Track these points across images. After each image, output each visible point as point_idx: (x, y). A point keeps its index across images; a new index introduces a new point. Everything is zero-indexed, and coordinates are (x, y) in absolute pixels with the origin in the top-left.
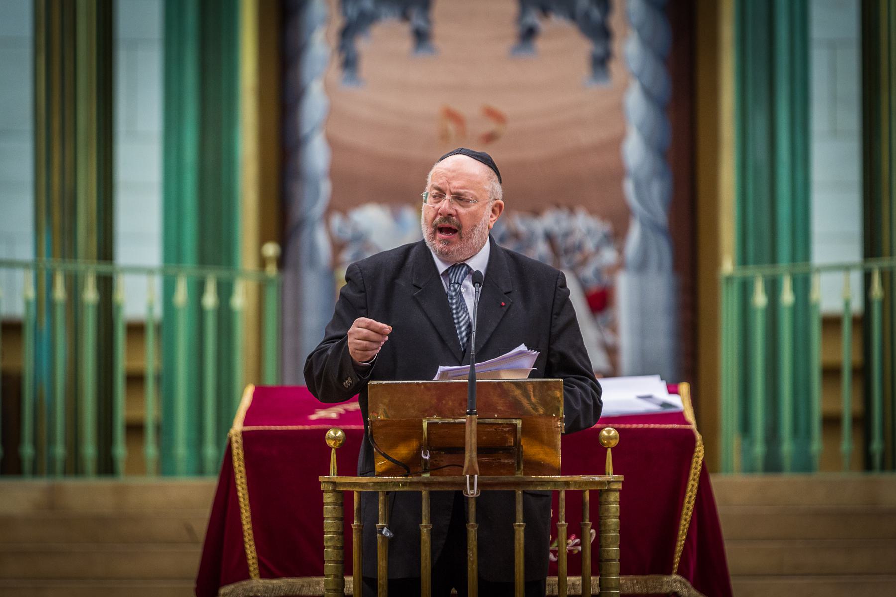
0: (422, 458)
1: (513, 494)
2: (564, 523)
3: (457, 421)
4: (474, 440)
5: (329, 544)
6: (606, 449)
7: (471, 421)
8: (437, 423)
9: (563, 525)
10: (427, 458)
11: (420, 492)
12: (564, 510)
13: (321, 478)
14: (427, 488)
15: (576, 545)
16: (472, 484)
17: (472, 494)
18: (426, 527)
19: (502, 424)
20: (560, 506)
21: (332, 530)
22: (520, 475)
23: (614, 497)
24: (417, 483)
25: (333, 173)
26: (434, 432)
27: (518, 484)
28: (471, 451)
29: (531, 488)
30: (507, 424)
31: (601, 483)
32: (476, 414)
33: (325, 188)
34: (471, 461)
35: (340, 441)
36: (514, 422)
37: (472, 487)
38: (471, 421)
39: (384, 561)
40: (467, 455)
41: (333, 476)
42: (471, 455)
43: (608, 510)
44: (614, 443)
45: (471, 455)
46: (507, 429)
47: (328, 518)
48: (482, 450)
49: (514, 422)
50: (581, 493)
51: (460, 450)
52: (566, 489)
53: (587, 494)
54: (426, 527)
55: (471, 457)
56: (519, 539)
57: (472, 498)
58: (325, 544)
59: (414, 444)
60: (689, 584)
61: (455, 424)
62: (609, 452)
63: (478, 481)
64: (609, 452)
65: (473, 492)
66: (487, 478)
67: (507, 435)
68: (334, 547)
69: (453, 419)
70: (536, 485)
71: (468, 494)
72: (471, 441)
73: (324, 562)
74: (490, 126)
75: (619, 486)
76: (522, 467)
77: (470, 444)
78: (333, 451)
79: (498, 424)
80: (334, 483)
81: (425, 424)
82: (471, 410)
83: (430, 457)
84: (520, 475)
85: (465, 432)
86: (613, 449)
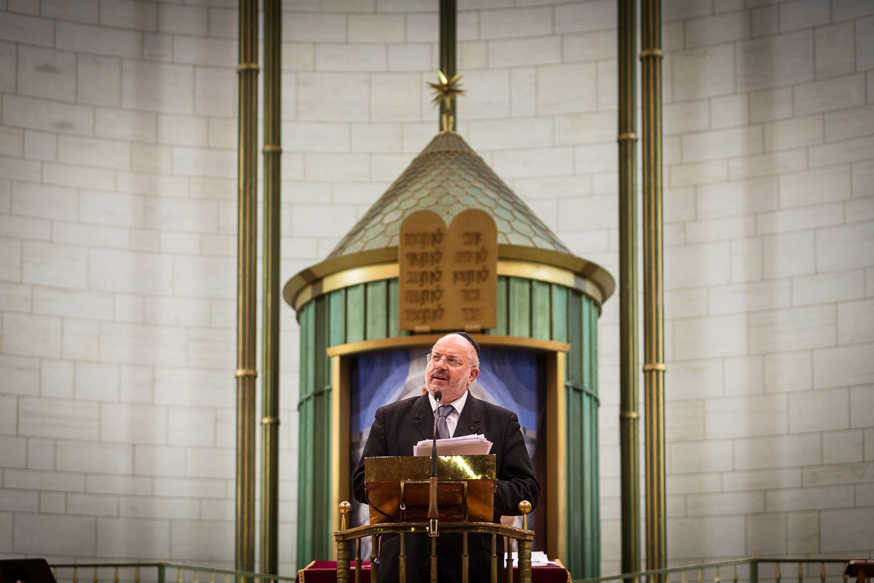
0: (401, 509)
1: (461, 535)
2: (495, 555)
3: (424, 482)
5: (340, 576)
7: (433, 481)
8: (410, 484)
9: (494, 557)
10: (404, 509)
11: (399, 534)
12: (495, 547)
14: (404, 531)
17: (434, 534)
18: (403, 556)
19: (454, 484)
20: (493, 544)
21: (342, 566)
26: (409, 493)
28: (433, 501)
29: (474, 531)
30: (458, 484)
32: (436, 476)
34: (433, 508)
35: (348, 509)
36: (462, 482)
37: (434, 530)
38: (433, 481)
39: (375, 581)
46: (457, 490)
49: (462, 482)
52: (496, 532)
54: (403, 556)
55: (433, 505)
56: (465, 565)
57: (434, 537)
58: (338, 576)
59: (396, 502)
61: (423, 484)
63: (438, 526)
65: (434, 533)
66: (444, 524)
67: (457, 495)
68: (344, 578)
69: (422, 481)
71: (431, 535)
76: (467, 518)
77: (432, 497)
79: (451, 484)
81: (402, 485)
82: (434, 474)
83: (406, 509)
84: (466, 522)
85: (429, 492)
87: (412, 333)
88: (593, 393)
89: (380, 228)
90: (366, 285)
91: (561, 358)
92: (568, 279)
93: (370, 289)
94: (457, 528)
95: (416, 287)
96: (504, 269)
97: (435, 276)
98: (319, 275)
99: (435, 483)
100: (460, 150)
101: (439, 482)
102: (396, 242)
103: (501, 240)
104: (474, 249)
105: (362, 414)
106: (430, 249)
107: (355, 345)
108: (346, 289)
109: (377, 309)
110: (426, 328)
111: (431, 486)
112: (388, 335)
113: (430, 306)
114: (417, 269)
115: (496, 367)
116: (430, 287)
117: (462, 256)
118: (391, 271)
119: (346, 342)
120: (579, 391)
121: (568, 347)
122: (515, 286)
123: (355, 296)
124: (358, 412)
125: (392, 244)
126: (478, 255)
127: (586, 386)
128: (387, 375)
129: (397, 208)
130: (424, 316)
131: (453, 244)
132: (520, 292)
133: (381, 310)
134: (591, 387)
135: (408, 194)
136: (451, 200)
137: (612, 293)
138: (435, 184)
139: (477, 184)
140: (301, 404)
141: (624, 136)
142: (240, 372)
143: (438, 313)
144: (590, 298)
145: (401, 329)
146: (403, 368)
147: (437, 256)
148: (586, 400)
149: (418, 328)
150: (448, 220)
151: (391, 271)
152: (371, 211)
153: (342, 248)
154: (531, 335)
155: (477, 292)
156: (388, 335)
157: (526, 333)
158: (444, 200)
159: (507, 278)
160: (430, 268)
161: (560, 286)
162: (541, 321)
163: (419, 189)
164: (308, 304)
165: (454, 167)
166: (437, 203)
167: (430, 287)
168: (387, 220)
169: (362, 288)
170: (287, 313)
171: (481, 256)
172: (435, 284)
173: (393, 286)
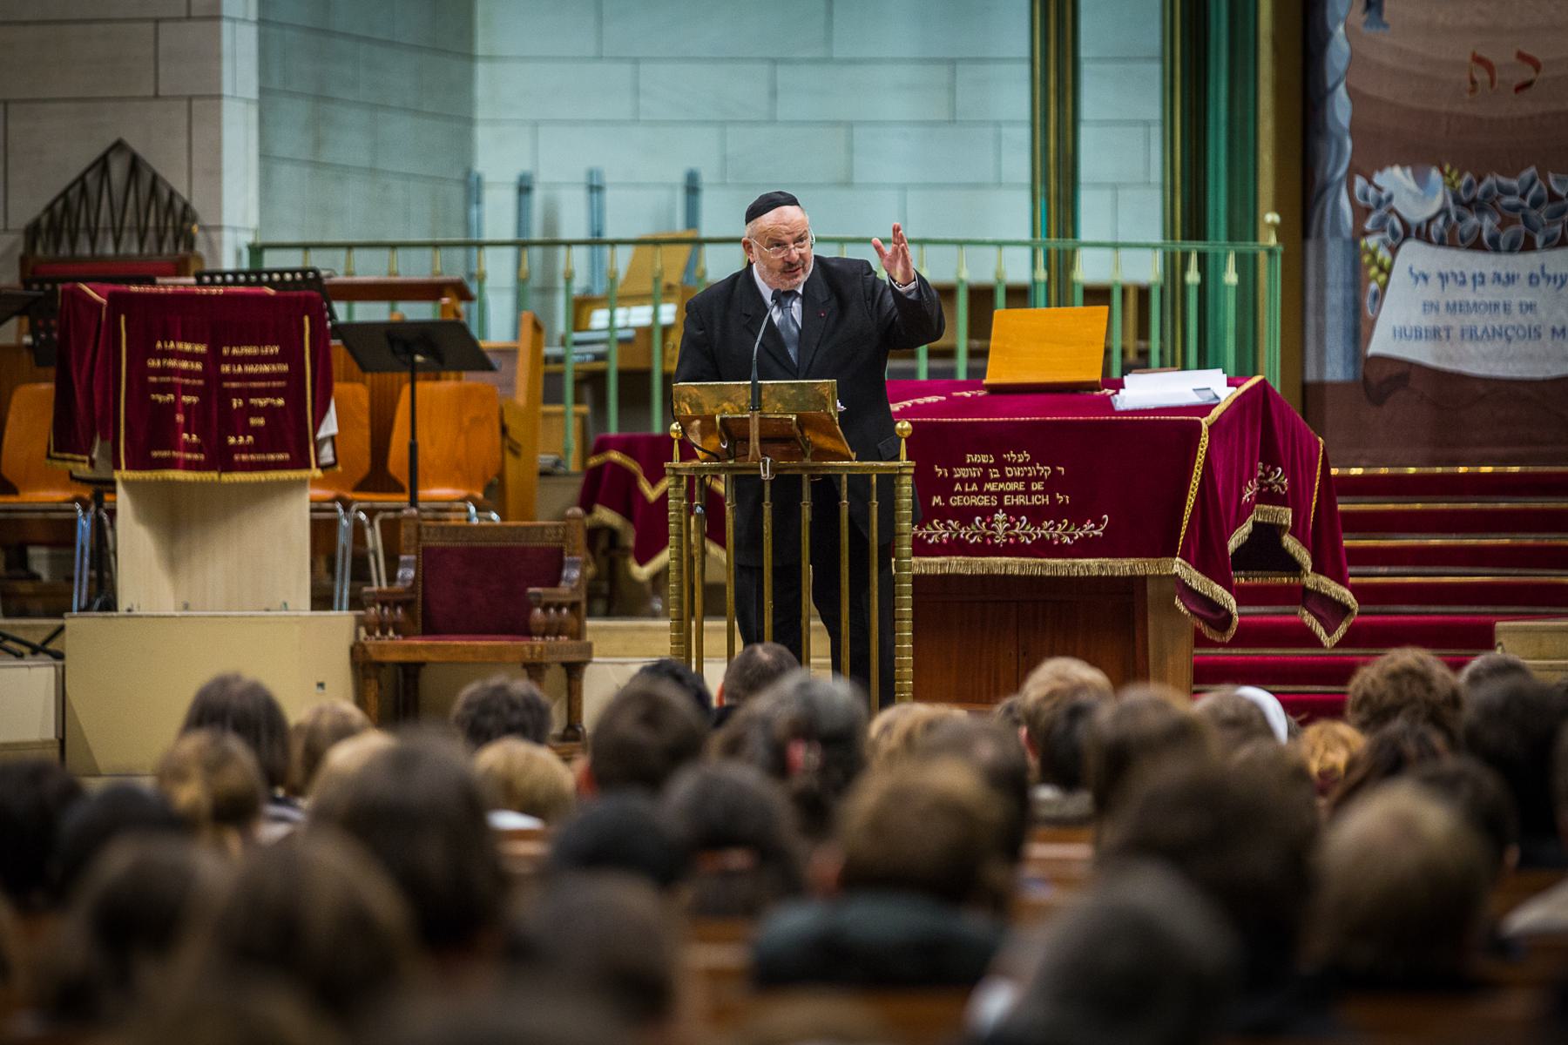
2: (845, 502)
4: (756, 432)
6: (901, 439)
9: (844, 504)
10: (725, 447)
13: (666, 465)
15: (1091, 529)
16: (765, 469)
18: (729, 505)
22: (807, 461)
23: (908, 480)
25: (1354, 131)
33: (1349, 144)
36: (790, 416)
37: (765, 472)
40: (751, 444)
41: (676, 463)
42: (755, 443)
43: (900, 491)
44: (907, 434)
45: (755, 443)
47: (671, 499)
48: (762, 440)
49: (790, 416)
53: (874, 477)
54: (729, 505)
60: (1190, 567)
62: (903, 441)
64: (903, 441)
65: (766, 475)
70: (819, 470)
72: (754, 432)
73: (668, 536)
74: (1528, 73)
75: (912, 471)
78: (676, 442)
80: (674, 469)
81: (718, 419)
82: (754, 407)
83: (728, 447)
84: (807, 461)
86: (907, 440)
99: (756, 419)
101: (763, 416)
111: (751, 421)
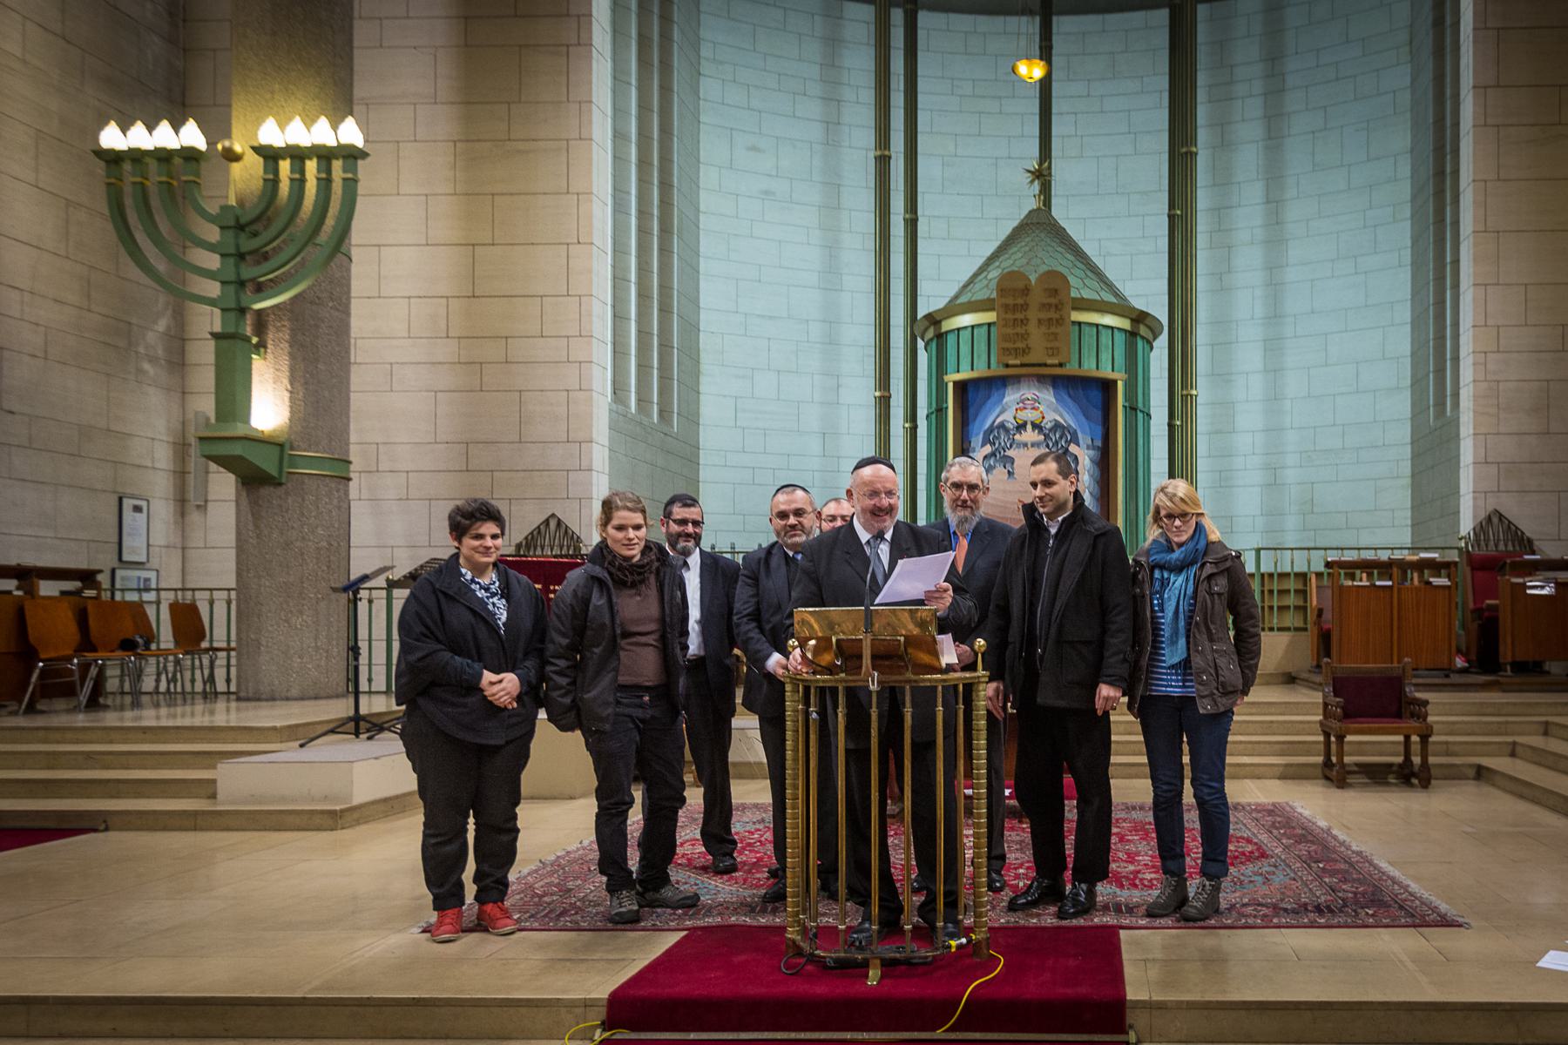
1: (904, 688)
4: (869, 652)
7: (866, 637)
16: (873, 681)
22: (909, 675)
24: (836, 681)
27: (909, 681)
31: (975, 678)
34: (867, 667)
37: (873, 684)
38: (866, 637)
40: (864, 661)
42: (867, 661)
43: (977, 696)
44: (983, 649)
45: (867, 661)
48: (874, 657)
50: (955, 687)
51: (860, 657)
65: (874, 687)
81: (834, 639)
86: (983, 655)
87: (1007, 366)
88: (1146, 410)
89: (985, 282)
90: (973, 327)
91: (1120, 384)
92: (1125, 324)
93: (976, 331)
94: (900, 681)
95: (1010, 331)
96: (1077, 316)
97: (1025, 322)
98: (938, 319)
100: (1047, 222)
102: (994, 295)
103: (1074, 294)
104: (1053, 301)
105: (970, 427)
106: (1020, 301)
107: (965, 375)
108: (959, 329)
109: (981, 347)
110: (1018, 362)
111: (864, 642)
112: (989, 367)
113: (1020, 345)
114: (1010, 316)
115: (1071, 392)
116: (1019, 330)
117: (1045, 306)
118: (990, 317)
119: (958, 371)
120: (1134, 409)
121: (1125, 376)
122: (1086, 329)
123: (965, 335)
124: (968, 425)
125: (992, 297)
126: (1056, 306)
127: (1140, 405)
128: (989, 397)
129: (998, 267)
130: (1017, 352)
131: (1037, 297)
132: (1089, 334)
133: (984, 347)
134: (1144, 406)
135: (1007, 256)
136: (1039, 261)
137: (1161, 333)
138: (1027, 248)
139: (1059, 249)
140: (927, 416)
141: (1172, 212)
142: (878, 394)
143: (1026, 351)
144: (1143, 338)
145: (998, 363)
146: (1001, 392)
147: (1025, 307)
148: (1140, 415)
149: (1011, 362)
150: (1033, 278)
151: (990, 317)
152: (980, 268)
153: (956, 297)
154: (1097, 368)
155: (1055, 335)
156: (989, 367)
157: (1094, 366)
158: (1033, 263)
159: (1080, 324)
160: (1019, 316)
161: (1119, 329)
162: (1105, 357)
163: (1015, 253)
164: (931, 340)
165: (1043, 235)
166: (1028, 263)
167: (1019, 330)
168: (990, 277)
169: (970, 329)
170: (921, 344)
171: (1058, 307)
172: (1024, 327)
173: (992, 329)
